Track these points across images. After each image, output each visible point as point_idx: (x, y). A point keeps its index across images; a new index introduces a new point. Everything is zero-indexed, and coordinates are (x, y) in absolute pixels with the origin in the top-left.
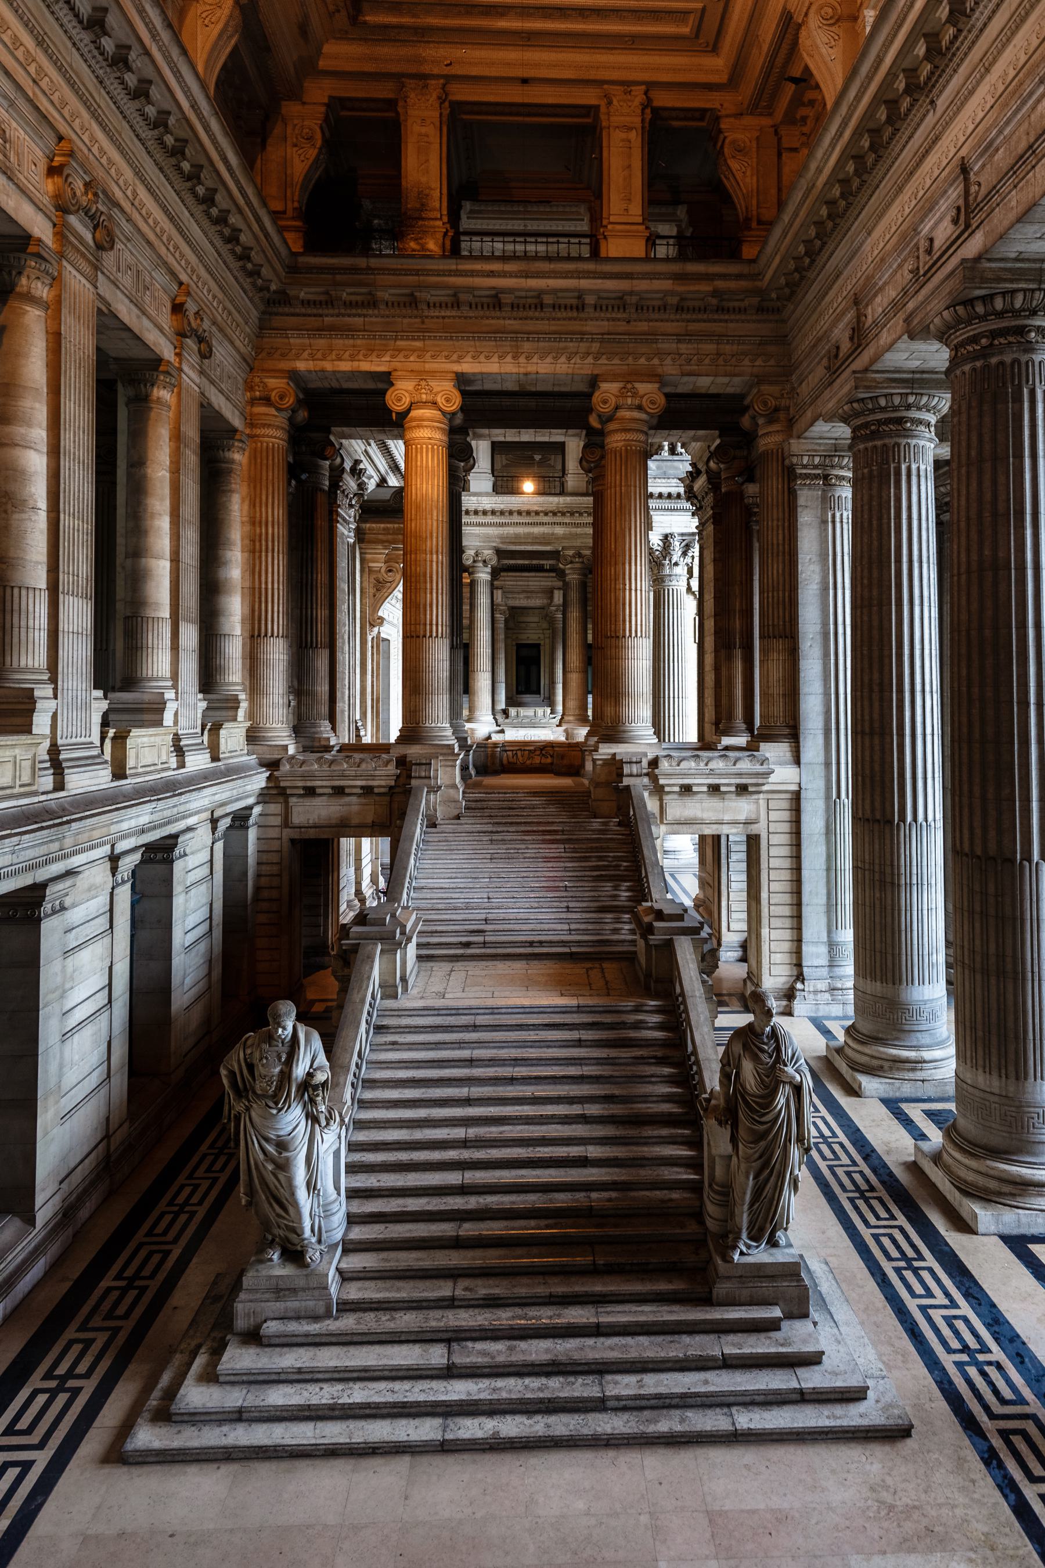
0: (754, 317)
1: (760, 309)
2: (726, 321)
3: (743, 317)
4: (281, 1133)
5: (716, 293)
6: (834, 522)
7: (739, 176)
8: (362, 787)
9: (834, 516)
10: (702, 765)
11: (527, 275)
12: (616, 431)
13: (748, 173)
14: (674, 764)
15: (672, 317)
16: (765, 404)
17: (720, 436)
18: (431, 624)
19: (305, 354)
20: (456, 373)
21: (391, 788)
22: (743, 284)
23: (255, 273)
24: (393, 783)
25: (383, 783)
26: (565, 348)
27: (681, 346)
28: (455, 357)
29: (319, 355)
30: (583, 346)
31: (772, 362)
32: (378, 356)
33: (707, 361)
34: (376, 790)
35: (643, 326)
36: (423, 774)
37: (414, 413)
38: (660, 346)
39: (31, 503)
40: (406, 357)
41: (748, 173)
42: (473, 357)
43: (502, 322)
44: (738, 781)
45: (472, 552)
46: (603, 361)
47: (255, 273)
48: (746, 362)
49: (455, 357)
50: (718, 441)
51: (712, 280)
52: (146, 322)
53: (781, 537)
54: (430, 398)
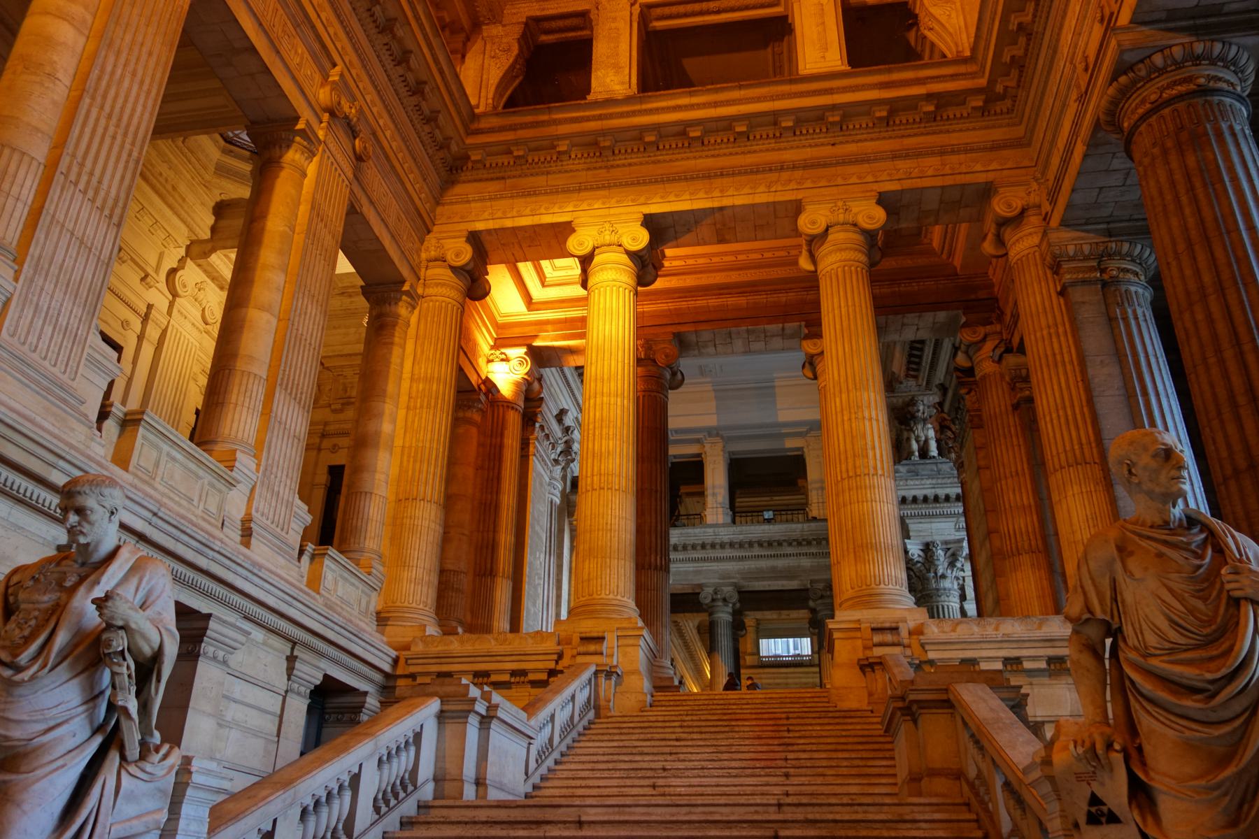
2: (948, 131)
4: (17, 733)
5: (929, 97)
6: (1125, 319)
7: (943, 19)
9: (1124, 313)
11: (716, 104)
12: (831, 253)
13: (954, 15)
14: (947, 629)
16: (1010, 206)
20: (646, 216)
23: (431, 119)
25: (540, 665)
37: (597, 259)
39: (48, 69)
41: (954, 15)
43: (693, 162)
44: (1051, 652)
45: (710, 590)
47: (431, 119)
51: (924, 84)
52: (278, 61)
53: (1056, 346)
54: (614, 239)
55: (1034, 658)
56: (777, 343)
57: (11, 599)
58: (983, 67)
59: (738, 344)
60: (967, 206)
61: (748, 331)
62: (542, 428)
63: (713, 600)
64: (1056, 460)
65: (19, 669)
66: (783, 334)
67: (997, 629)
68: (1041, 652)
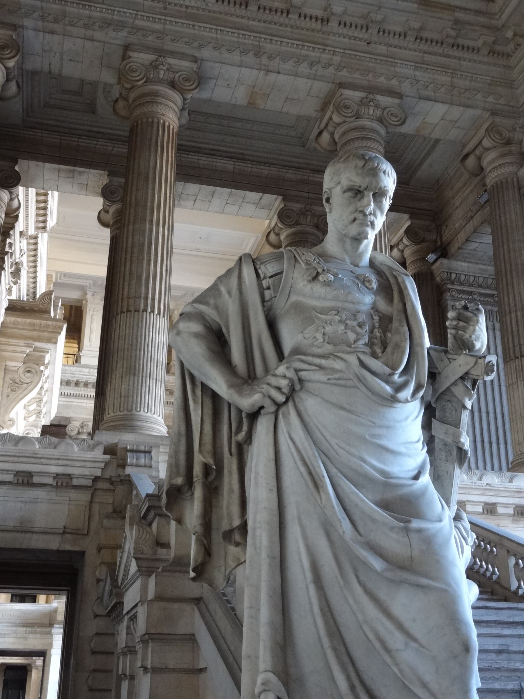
0: (485, 59)
1: (492, 52)
3: (476, 57)
8: (57, 476)
10: (475, 479)
15: (411, 45)
16: (501, 134)
17: (411, 218)
18: (153, 300)
19: (36, 15)
21: (96, 479)
22: (481, 19)
24: (99, 473)
25: (87, 472)
26: (307, 56)
27: (417, 73)
28: (196, 44)
29: (50, 18)
30: (325, 56)
31: (502, 101)
32: (114, 30)
33: (443, 89)
34: (75, 482)
35: (383, 49)
36: (142, 461)
38: (398, 70)
40: (143, 35)
42: (215, 48)
46: (344, 73)
48: (479, 96)
49: (196, 44)
50: (408, 223)
51: (454, 11)
55: (506, 505)
56: (249, 209)
57: (268, 294)
58: (502, 11)
59: (217, 202)
60: (459, 127)
61: (230, 194)
62: (11, 244)
63: (79, 433)
64: (517, 349)
65: (399, 388)
66: (257, 205)
67: (480, 479)
68: (511, 501)
